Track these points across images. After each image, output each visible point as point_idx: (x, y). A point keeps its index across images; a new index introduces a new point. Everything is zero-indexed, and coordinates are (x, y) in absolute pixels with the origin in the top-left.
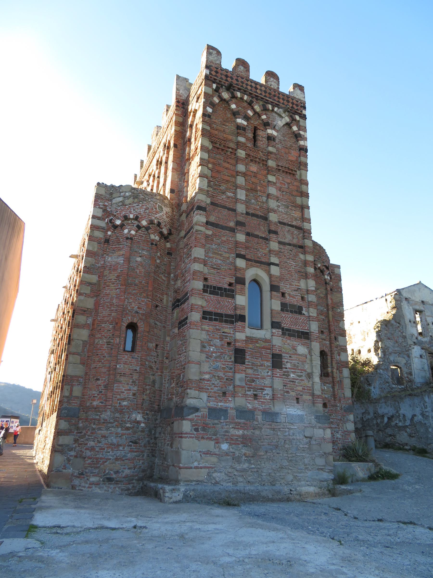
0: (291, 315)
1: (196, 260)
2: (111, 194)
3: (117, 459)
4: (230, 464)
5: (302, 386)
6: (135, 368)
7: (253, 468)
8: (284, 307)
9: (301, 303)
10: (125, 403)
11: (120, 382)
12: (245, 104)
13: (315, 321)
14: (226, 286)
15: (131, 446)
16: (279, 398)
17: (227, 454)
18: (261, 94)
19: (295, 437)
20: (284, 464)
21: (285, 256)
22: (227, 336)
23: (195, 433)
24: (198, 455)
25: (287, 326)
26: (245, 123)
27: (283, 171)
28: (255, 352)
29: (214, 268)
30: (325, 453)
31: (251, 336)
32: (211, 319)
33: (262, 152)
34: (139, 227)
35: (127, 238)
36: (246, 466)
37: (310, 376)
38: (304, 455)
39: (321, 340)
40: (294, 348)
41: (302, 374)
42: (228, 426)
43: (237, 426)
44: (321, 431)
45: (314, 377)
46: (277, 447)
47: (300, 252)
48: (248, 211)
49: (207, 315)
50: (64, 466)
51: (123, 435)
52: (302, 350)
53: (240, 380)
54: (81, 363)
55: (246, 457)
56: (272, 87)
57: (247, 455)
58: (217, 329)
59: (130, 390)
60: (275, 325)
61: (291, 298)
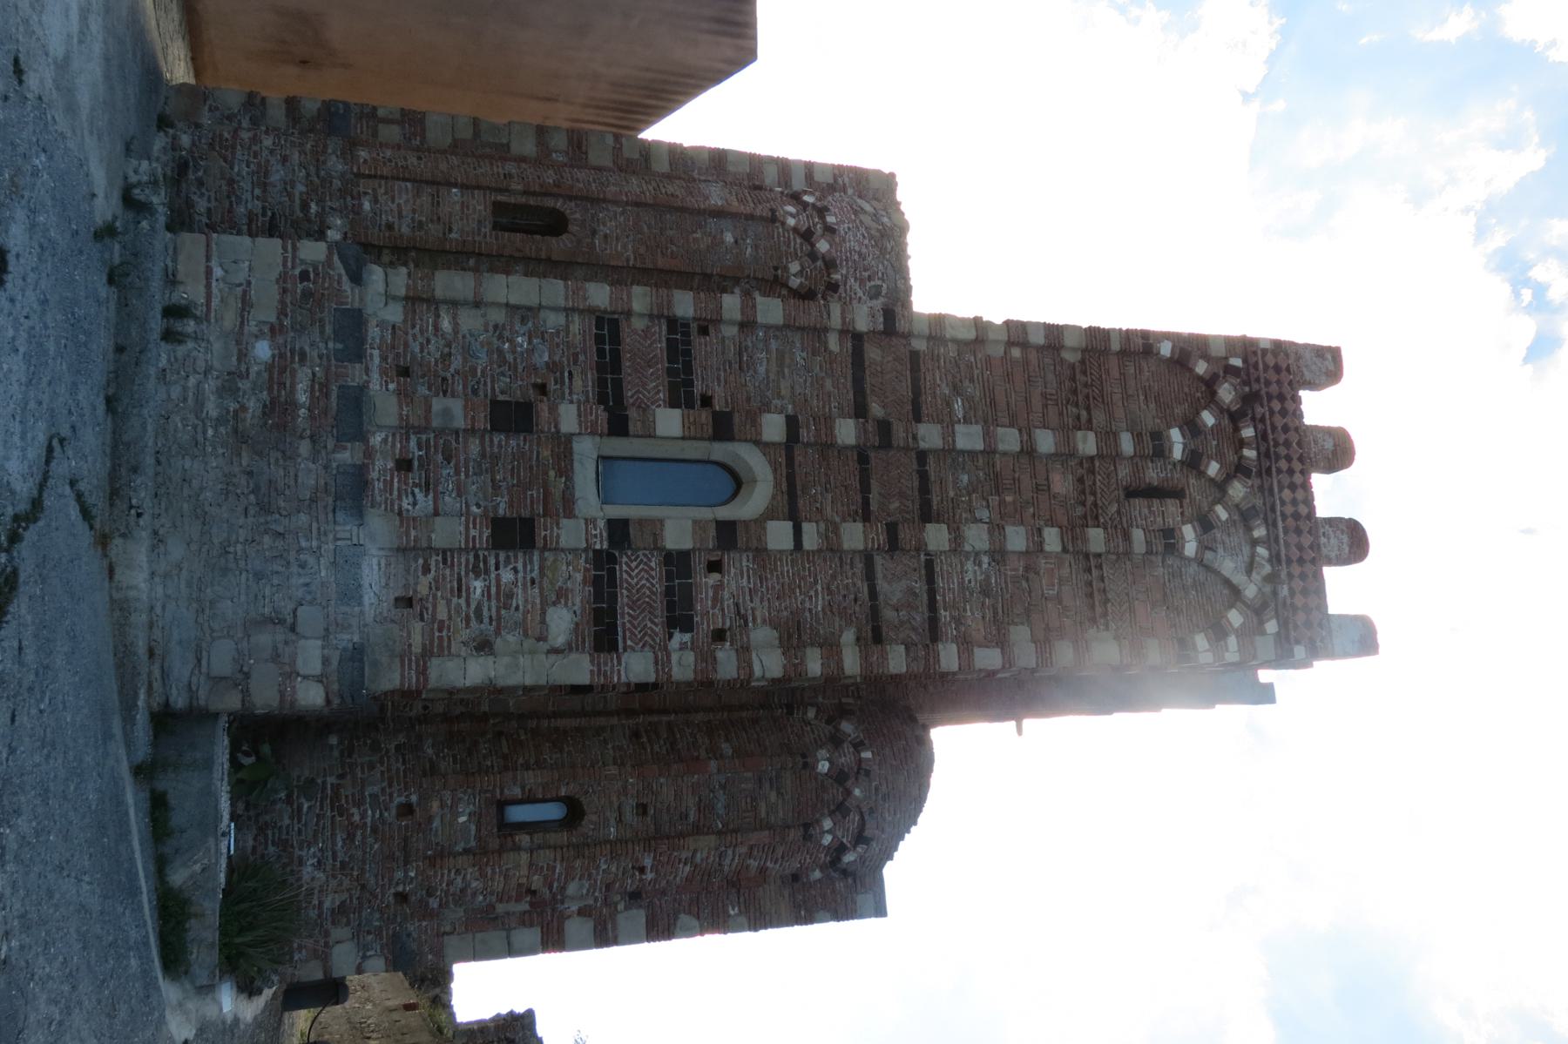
0: (659, 588)
3: (231, 182)
4: (216, 364)
5: (450, 618)
6: (455, 228)
7: (205, 432)
8: (678, 563)
9: (704, 627)
10: (367, 206)
11: (418, 194)
12: (1231, 457)
13: (657, 671)
14: (698, 388)
15: (264, 215)
16: (407, 534)
17: (242, 355)
18: (1283, 503)
19: (294, 569)
20: (214, 530)
21: (834, 577)
22: (563, 383)
23: (297, 272)
24: (241, 277)
25: (625, 576)
26: (1177, 453)
27: (1090, 584)
28: (531, 467)
29: (740, 355)
30: (247, 676)
31: (576, 457)
32: (599, 339)
33: (1118, 512)
36: (212, 409)
37: (484, 647)
38: (243, 598)
39: (616, 805)
40: (562, 595)
41: (486, 620)
42: (317, 361)
43: (320, 389)
44: (315, 667)
45: (481, 660)
46: (265, 508)
47: (859, 630)
48: (931, 460)
49: (608, 328)
50: (217, 108)
51: (290, 195)
52: (561, 623)
53: (446, 412)
54: (454, 140)
55: (236, 412)
56: (1323, 540)
57: (242, 415)
58: (576, 355)
59: (400, 216)
60: (619, 530)
61: (711, 594)
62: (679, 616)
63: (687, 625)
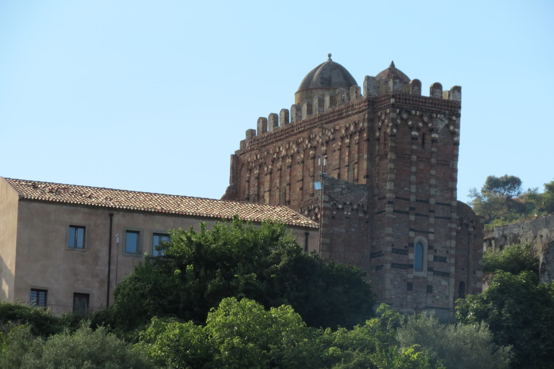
1: (388, 235)
2: (332, 184)
34: (352, 210)
35: (347, 217)
62: (444, 260)
63: (445, 258)
